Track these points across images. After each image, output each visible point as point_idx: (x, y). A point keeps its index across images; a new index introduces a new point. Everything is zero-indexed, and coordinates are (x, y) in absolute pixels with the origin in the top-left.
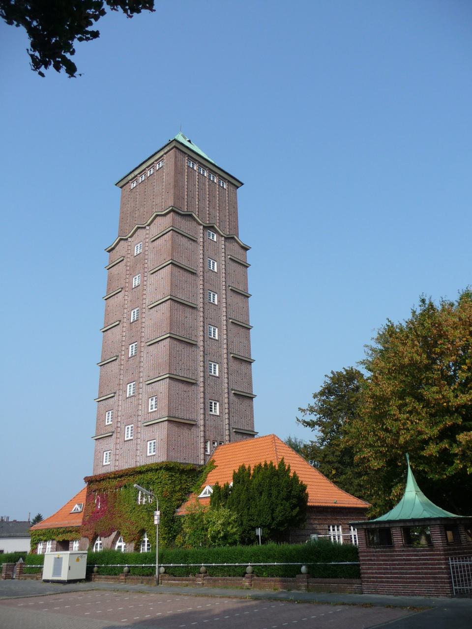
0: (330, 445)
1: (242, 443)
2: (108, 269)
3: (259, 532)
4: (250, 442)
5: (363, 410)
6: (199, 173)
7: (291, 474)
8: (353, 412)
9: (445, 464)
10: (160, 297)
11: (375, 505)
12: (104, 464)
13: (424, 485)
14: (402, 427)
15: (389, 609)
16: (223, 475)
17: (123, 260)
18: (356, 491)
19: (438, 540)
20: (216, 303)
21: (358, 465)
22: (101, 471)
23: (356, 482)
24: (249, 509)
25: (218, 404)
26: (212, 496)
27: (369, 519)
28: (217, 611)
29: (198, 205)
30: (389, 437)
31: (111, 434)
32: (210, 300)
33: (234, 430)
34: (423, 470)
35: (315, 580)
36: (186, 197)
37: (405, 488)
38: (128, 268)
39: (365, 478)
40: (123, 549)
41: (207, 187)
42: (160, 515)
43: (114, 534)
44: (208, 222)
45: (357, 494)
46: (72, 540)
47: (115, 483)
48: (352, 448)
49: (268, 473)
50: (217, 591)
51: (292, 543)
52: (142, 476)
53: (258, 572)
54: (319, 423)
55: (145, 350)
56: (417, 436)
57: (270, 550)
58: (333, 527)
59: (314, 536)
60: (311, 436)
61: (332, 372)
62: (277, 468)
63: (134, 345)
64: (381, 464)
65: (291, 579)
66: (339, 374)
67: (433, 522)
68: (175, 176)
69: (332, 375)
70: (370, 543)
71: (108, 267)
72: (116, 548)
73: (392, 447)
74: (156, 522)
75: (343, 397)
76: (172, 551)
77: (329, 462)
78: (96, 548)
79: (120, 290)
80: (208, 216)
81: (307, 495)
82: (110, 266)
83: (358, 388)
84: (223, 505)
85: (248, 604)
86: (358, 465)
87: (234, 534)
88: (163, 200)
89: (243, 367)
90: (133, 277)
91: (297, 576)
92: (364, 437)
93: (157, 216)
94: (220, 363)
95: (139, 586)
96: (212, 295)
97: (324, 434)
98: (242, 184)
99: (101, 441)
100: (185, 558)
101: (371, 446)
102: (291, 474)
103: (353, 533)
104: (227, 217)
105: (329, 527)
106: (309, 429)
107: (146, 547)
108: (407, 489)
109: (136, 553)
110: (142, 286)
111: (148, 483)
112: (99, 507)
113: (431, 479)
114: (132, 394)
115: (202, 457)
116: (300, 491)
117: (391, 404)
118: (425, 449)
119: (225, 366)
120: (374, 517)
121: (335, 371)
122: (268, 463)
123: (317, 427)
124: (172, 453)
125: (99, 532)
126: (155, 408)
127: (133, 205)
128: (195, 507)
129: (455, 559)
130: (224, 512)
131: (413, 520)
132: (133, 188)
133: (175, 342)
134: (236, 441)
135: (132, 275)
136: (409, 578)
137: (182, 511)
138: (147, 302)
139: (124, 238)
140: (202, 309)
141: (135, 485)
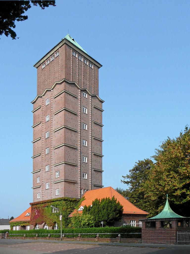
0: (135, 191)
1: (97, 190)
2: (33, 113)
3: (102, 223)
4: (100, 189)
5: (151, 177)
6: (78, 59)
7: (117, 202)
8: (146, 177)
9: (183, 198)
10: (59, 126)
11: (151, 213)
12: (38, 198)
13: (173, 206)
14: (167, 184)
15: (151, 248)
16: (88, 202)
17: (40, 108)
18: (144, 208)
19: (174, 225)
20: (86, 129)
21: (146, 199)
22: (36, 201)
23: (144, 205)
24: (98, 215)
25: (86, 174)
26: (84, 210)
27: (148, 218)
28: (85, 249)
29: (78, 78)
30: (160, 188)
31: (40, 186)
32: (84, 128)
33: (93, 185)
34: (173, 201)
35: (124, 239)
36: (72, 73)
37: (164, 207)
38: (43, 112)
39: (148, 203)
40: (47, 229)
41: (83, 67)
42: (62, 217)
43: (43, 224)
44: (83, 88)
45: (144, 209)
46: (27, 226)
47: (43, 205)
48: (144, 192)
49: (107, 201)
50: (85, 242)
51: (115, 226)
52: (54, 203)
53: (101, 236)
54: (131, 182)
55: (53, 151)
56: (173, 187)
57: (106, 229)
58: (133, 221)
59: (124, 224)
60: (126, 187)
61: (139, 161)
62: (111, 200)
63: (48, 149)
64: (156, 198)
65: (114, 238)
66: (142, 162)
67: (173, 219)
68: (66, 61)
69: (139, 162)
70: (146, 227)
71: (33, 112)
72: (45, 228)
73: (161, 191)
74: (60, 219)
75: (143, 171)
76: (67, 229)
77: (133, 197)
78: (37, 228)
79: (40, 123)
80: (83, 84)
81: (123, 210)
82: (34, 111)
83: (150, 168)
84: (88, 213)
85: (97, 246)
86: (146, 199)
87: (92, 223)
88: (60, 75)
89: (99, 158)
90: (46, 116)
91: (117, 237)
92: (150, 187)
93: (57, 84)
94: (88, 157)
95: (54, 241)
96: (84, 126)
97: (132, 186)
98: (102, 66)
99: (35, 189)
100: (73, 231)
101: (152, 191)
102: (117, 202)
103: (140, 223)
104: (93, 85)
105: (131, 221)
106: (126, 184)
107: (57, 228)
108: (165, 208)
109: (53, 230)
110: (51, 121)
111: (57, 205)
112: (37, 214)
113: (176, 204)
114: (48, 170)
115: (79, 195)
116: (120, 208)
117: (163, 174)
118: (175, 193)
119: (90, 158)
120: (150, 217)
121: (140, 160)
122: (108, 198)
123: (130, 184)
124: (67, 194)
125: (37, 223)
126: (59, 176)
127: (44, 78)
128: (76, 214)
129: (180, 232)
130: (88, 216)
131: (166, 219)
132: (43, 68)
133: (67, 148)
134: (94, 189)
135: (45, 115)
136: (160, 238)
137: (71, 215)
138: (53, 129)
139: (40, 96)
140: (79, 132)
141: (51, 206)
